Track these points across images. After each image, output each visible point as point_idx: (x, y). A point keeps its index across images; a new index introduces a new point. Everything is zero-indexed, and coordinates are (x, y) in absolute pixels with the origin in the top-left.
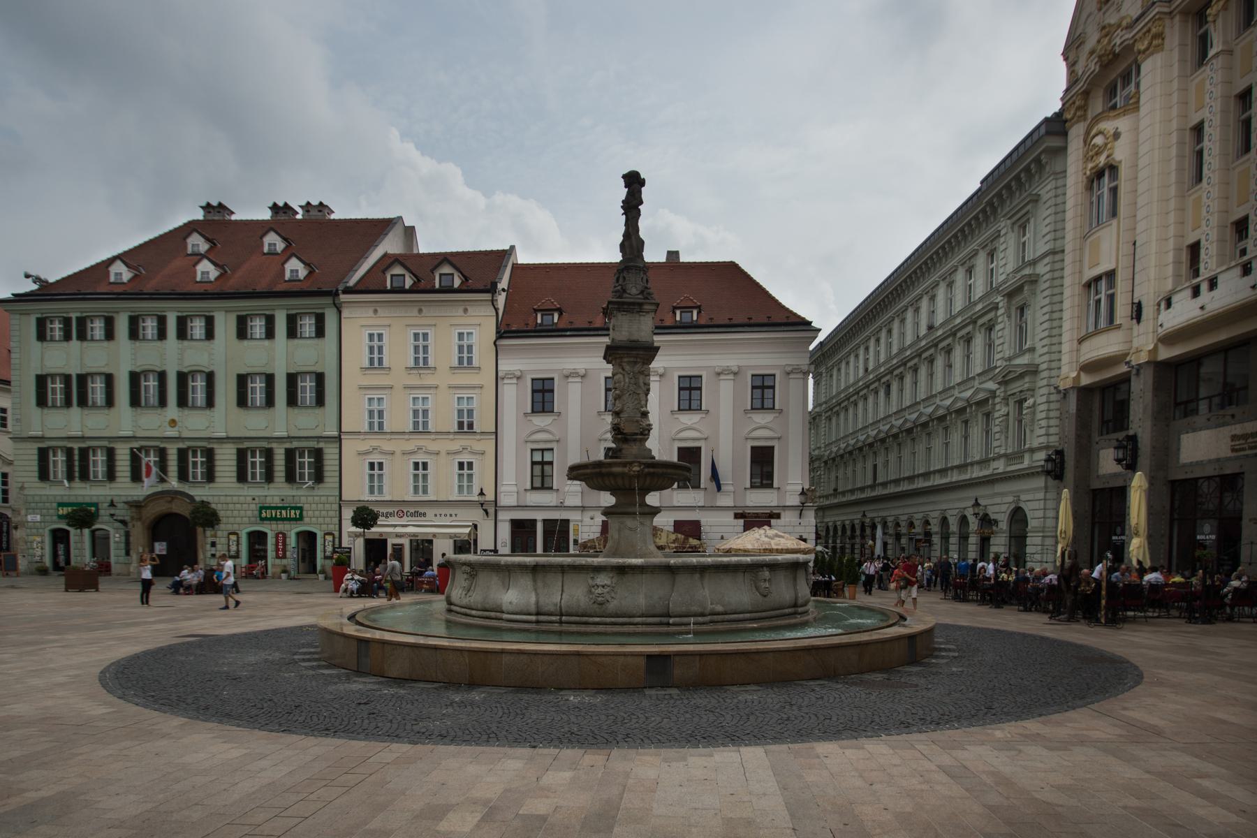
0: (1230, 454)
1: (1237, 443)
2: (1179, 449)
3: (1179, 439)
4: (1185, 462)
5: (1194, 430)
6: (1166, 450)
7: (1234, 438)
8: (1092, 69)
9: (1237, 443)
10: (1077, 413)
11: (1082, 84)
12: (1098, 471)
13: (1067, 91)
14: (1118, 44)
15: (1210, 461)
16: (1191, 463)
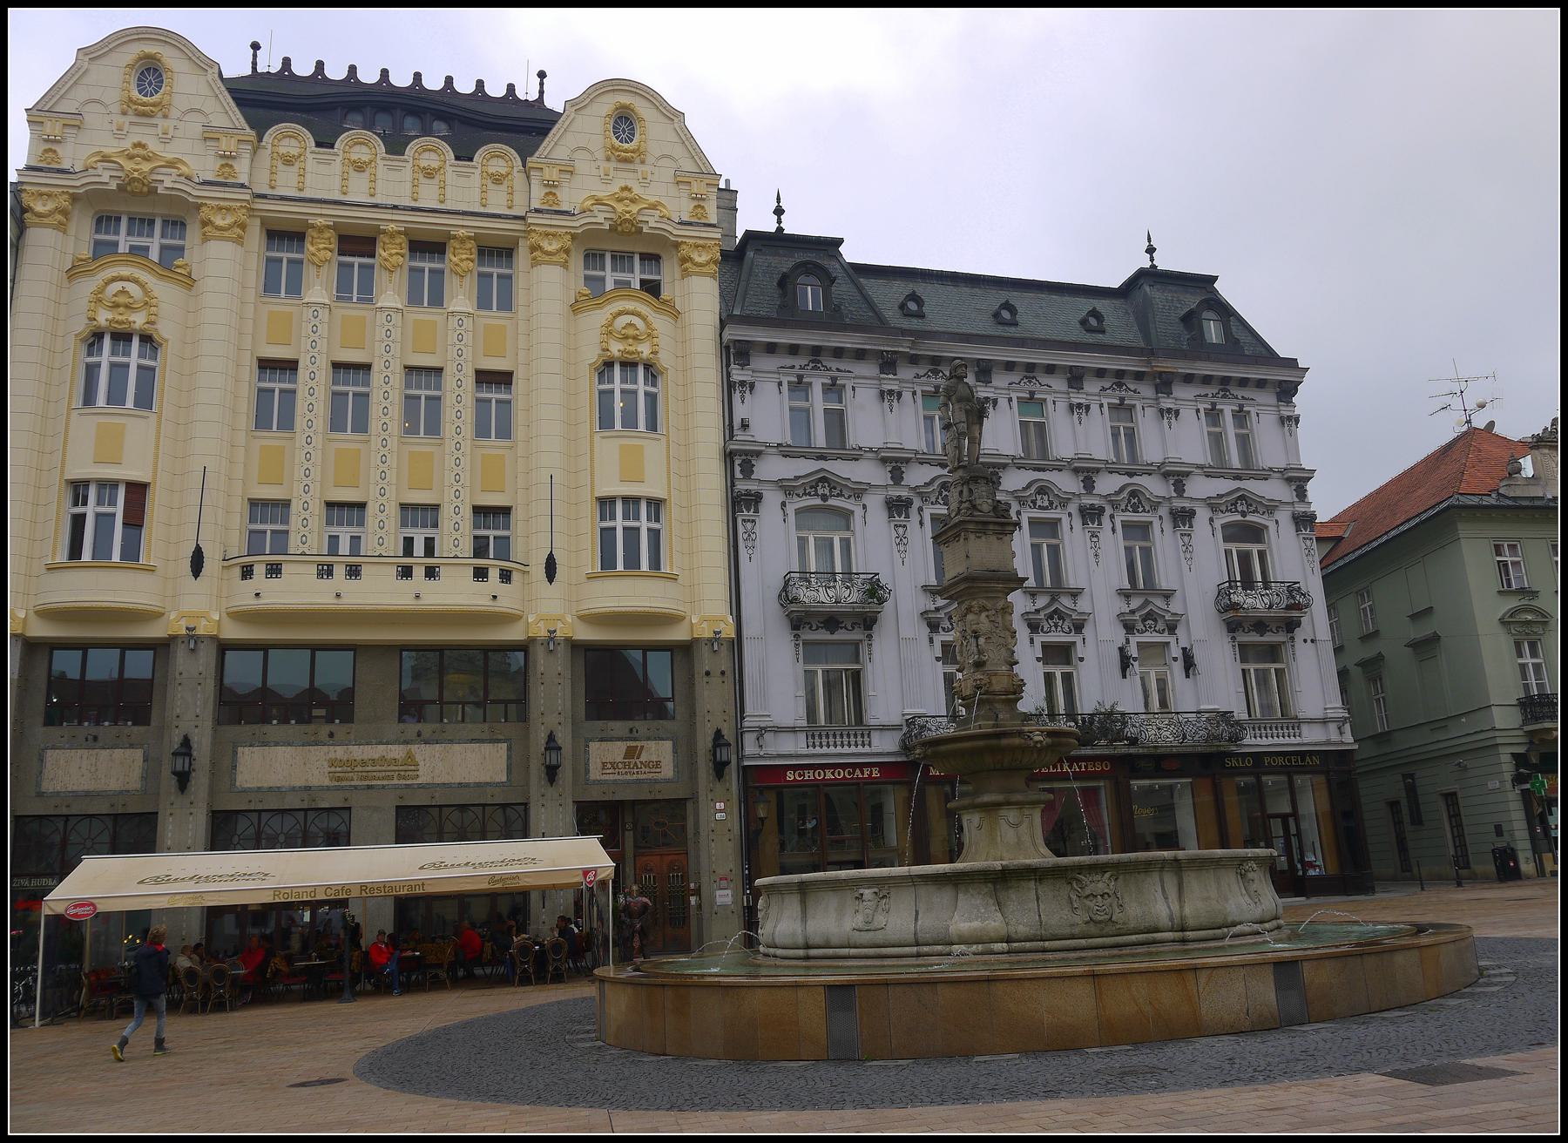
0: (327, 782)
1: (339, 769)
2: (234, 767)
3: (235, 753)
4: (246, 786)
5: (265, 744)
6: (224, 766)
7: (332, 763)
8: (106, 180)
9: (339, 769)
10: (18, 679)
11: (78, 183)
12: (38, 784)
13: (29, 168)
14: (168, 184)
15: (293, 789)
16: (259, 788)
